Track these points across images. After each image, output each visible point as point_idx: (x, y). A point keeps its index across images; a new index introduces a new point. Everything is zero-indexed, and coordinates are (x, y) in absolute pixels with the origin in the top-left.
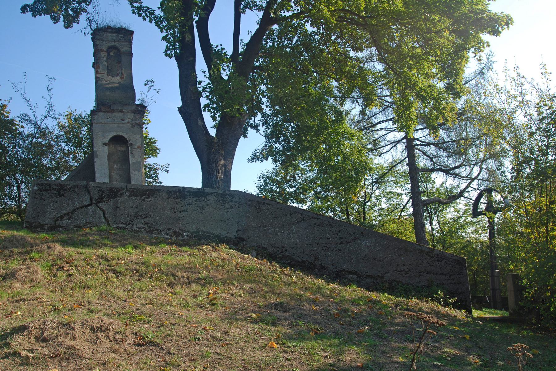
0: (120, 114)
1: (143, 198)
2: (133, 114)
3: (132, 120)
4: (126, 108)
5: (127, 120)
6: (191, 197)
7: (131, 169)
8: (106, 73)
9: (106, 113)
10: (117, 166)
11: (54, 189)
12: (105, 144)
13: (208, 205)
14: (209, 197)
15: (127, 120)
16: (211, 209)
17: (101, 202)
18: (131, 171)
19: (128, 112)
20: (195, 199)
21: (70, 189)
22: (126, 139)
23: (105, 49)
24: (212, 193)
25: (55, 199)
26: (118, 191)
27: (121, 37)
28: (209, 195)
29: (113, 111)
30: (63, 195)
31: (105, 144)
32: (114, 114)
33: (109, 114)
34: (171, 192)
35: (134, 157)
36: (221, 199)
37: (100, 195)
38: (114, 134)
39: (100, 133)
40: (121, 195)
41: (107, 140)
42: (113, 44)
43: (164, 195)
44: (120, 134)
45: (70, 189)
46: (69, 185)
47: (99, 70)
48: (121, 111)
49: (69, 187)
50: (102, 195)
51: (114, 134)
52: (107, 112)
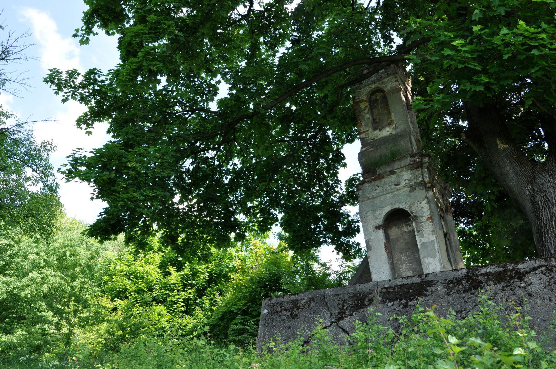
0: (393, 178)
1: (403, 301)
2: (409, 172)
3: (410, 180)
4: (396, 165)
5: (403, 183)
7: (421, 256)
8: (370, 129)
9: (373, 183)
10: (406, 256)
11: (286, 310)
12: (378, 228)
13: (530, 295)
14: (532, 278)
15: (403, 183)
16: (539, 302)
17: (342, 318)
18: (422, 259)
19: (402, 171)
20: (499, 286)
21: (304, 305)
22: (407, 211)
23: (364, 98)
24: (535, 269)
25: (287, 323)
26: (365, 296)
27: (382, 73)
29: (381, 177)
30: (296, 315)
31: (378, 228)
32: (383, 180)
33: (377, 183)
34: (451, 282)
37: (341, 306)
38: (389, 210)
39: (369, 214)
40: (371, 301)
41: (380, 221)
42: (373, 86)
43: (440, 289)
44: (397, 206)
46: (303, 299)
47: (362, 129)
48: (392, 173)
49: (303, 302)
50: (343, 306)
51: (388, 209)
52: (374, 180)
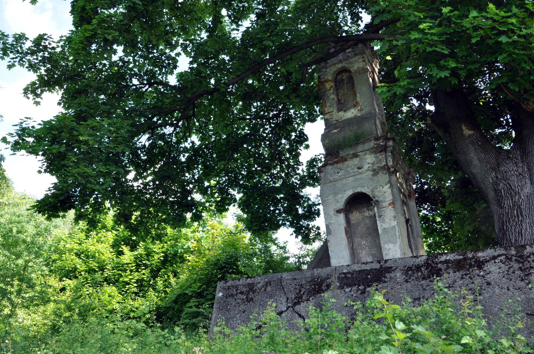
0: (356, 161)
1: (361, 287)
2: (373, 156)
3: (373, 164)
4: (360, 148)
5: (366, 167)
6: (451, 271)
7: (382, 242)
8: (335, 111)
9: (335, 165)
10: (366, 241)
11: (242, 293)
12: (339, 211)
13: (489, 284)
14: (491, 267)
15: (366, 167)
16: (497, 290)
17: (298, 303)
18: (382, 245)
19: (365, 154)
20: (458, 274)
21: (260, 289)
22: (369, 196)
23: (330, 78)
24: (494, 258)
25: (242, 307)
26: (323, 281)
27: (349, 52)
28: (487, 261)
29: (344, 160)
30: (252, 299)
31: (339, 211)
32: (346, 163)
33: (340, 165)
34: (410, 269)
35: (384, 222)
36: (516, 266)
37: (298, 291)
38: (351, 194)
39: (330, 197)
40: (328, 286)
41: (341, 205)
42: (340, 66)
43: (398, 275)
44: (359, 190)
45: (260, 289)
46: (260, 283)
47: (326, 109)
48: (356, 156)
49: (259, 286)
50: (300, 291)
51: (349, 193)
52: (337, 162)
